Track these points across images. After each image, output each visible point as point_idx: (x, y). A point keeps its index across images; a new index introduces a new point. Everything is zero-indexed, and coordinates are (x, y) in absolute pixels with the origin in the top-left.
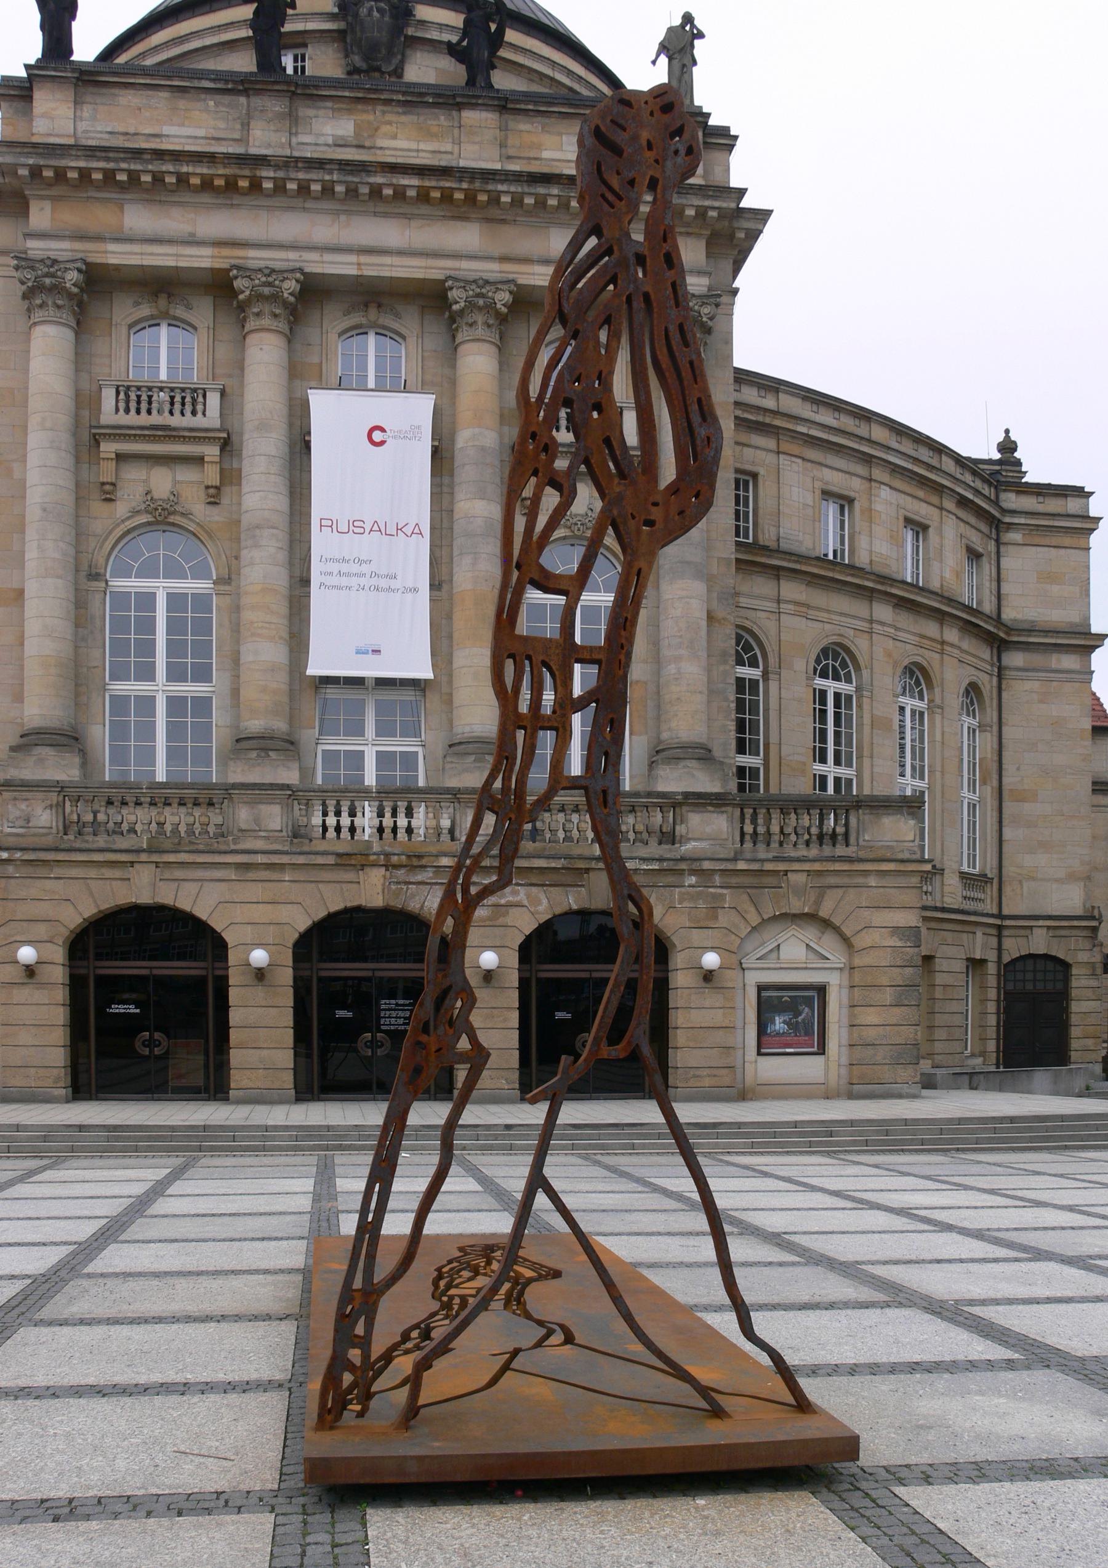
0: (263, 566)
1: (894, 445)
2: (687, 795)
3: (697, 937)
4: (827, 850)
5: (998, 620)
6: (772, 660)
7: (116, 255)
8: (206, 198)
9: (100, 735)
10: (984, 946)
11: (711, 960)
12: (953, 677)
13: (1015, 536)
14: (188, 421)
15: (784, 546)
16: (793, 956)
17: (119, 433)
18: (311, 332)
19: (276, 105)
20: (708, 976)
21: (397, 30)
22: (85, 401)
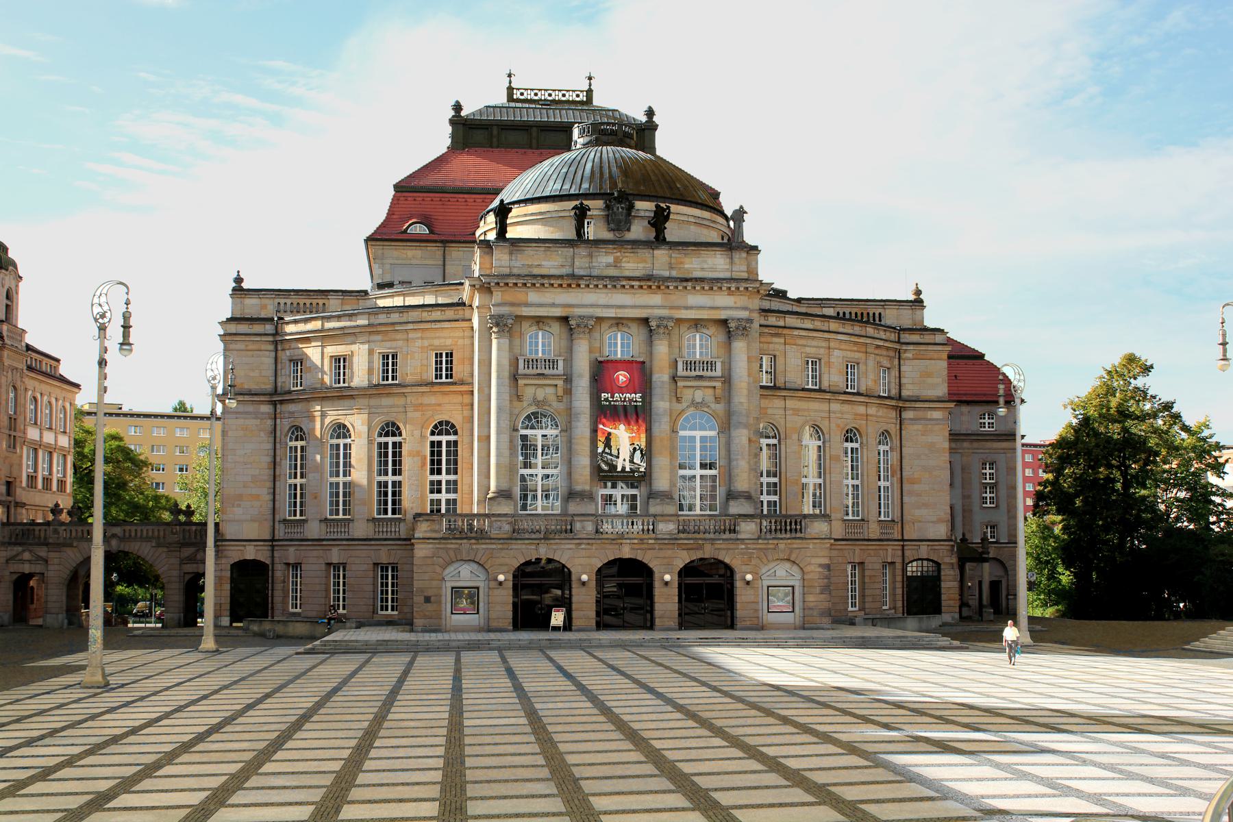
1: (841, 330)
2: (740, 515)
3: (744, 568)
4: (793, 535)
5: (900, 398)
6: (783, 436)
7: (526, 311)
8: (559, 290)
10: (893, 556)
11: (749, 577)
12: (872, 432)
13: (909, 355)
14: (551, 372)
15: (788, 386)
17: (526, 376)
18: (596, 335)
19: (582, 251)
20: (748, 583)
21: (629, 214)
22: (514, 363)
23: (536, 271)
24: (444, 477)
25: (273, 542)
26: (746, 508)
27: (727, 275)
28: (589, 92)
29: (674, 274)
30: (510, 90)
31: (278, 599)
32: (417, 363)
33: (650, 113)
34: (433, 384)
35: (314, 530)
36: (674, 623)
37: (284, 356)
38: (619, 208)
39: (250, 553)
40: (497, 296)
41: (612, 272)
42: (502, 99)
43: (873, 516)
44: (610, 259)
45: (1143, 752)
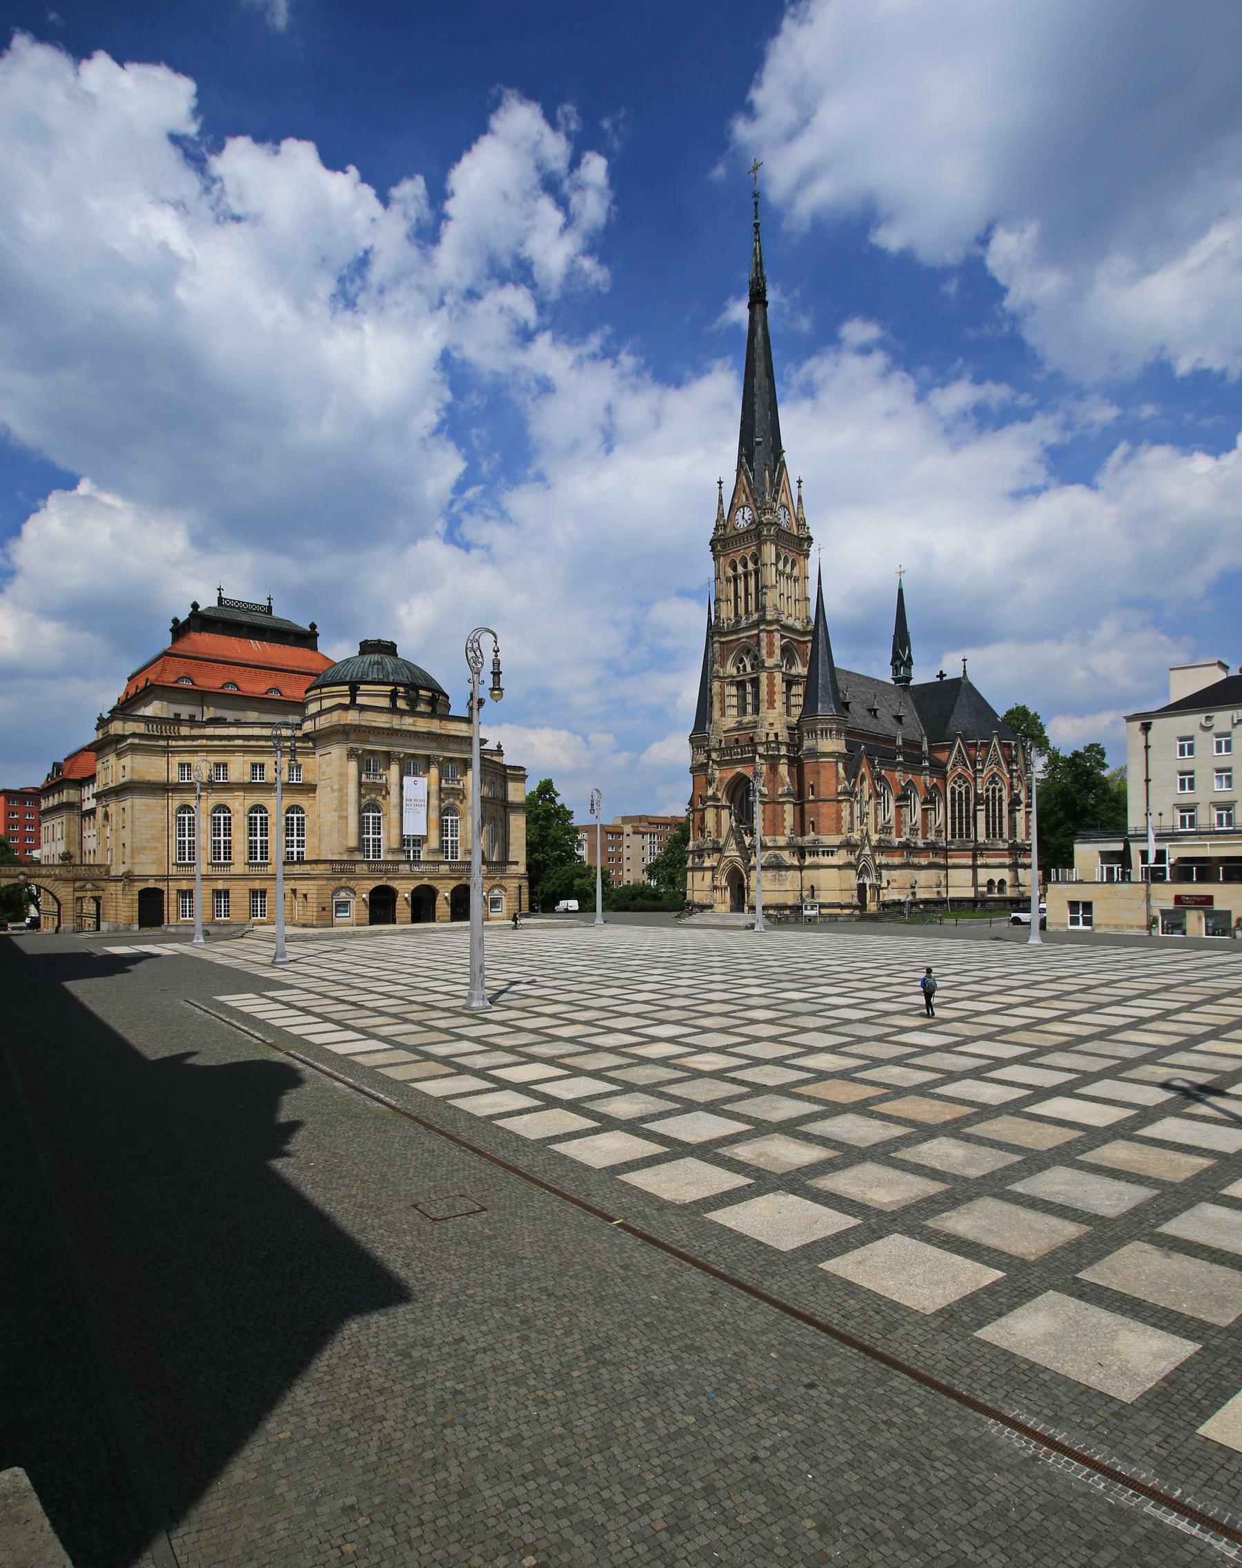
24: (295, 838)
25: (167, 878)
28: (270, 608)
29: (443, 732)
30: (220, 599)
33: (313, 626)
39: (151, 884)
42: (215, 604)
45: (436, 992)
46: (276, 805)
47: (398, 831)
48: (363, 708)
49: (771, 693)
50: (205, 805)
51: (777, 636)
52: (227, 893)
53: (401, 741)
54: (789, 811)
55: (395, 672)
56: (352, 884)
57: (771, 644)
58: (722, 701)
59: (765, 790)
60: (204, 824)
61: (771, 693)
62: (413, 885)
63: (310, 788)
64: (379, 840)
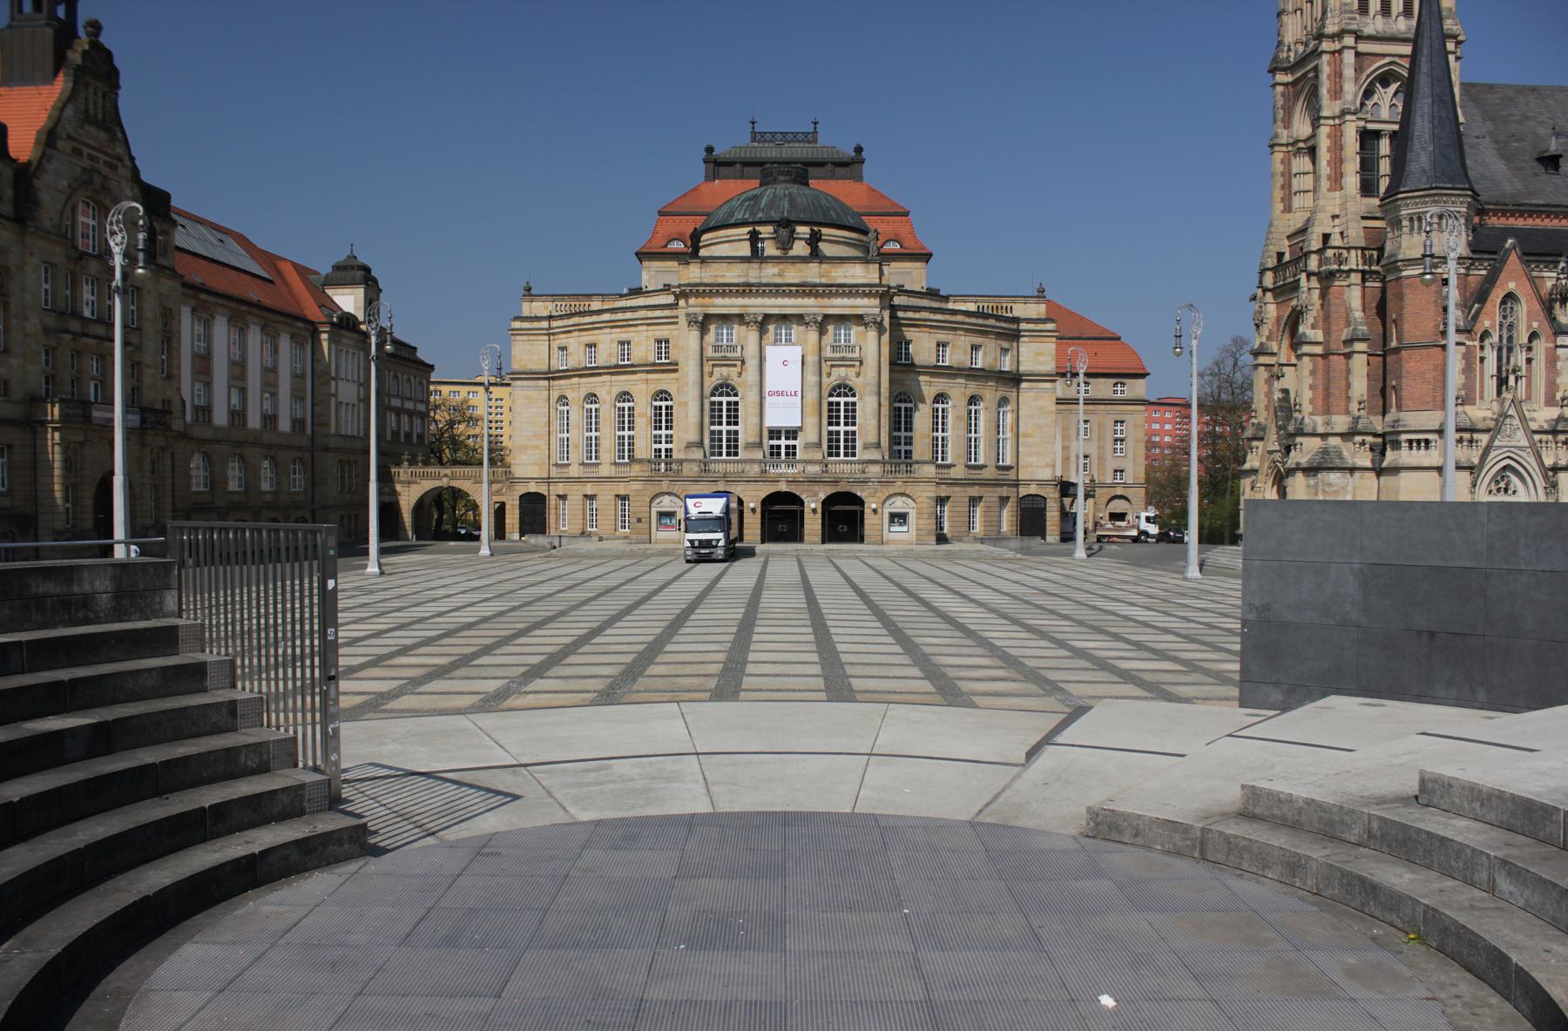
0: (752, 396)
7: (712, 311)
9: (707, 442)
16: (899, 505)
19: (756, 266)
23: (721, 281)
24: (664, 432)
25: (548, 480)
26: (875, 455)
27: (864, 281)
28: (815, 132)
29: (824, 281)
30: (754, 134)
31: (552, 521)
32: (643, 347)
33: (859, 150)
34: (654, 364)
35: (575, 471)
36: (819, 538)
37: (556, 343)
38: (783, 232)
39: (532, 488)
40: (692, 301)
41: (778, 280)
42: (745, 140)
43: (992, 463)
44: (776, 270)
46: (642, 388)
47: (756, 420)
48: (704, 260)
49: (1337, 162)
50: (576, 389)
51: (1349, 57)
52: (591, 498)
53: (759, 301)
54: (1359, 364)
55: (772, 204)
56: (677, 488)
57: (1338, 75)
58: (1287, 186)
59: (1319, 335)
60: (577, 416)
61: (1337, 162)
62: (766, 490)
63: (672, 368)
64: (736, 433)
